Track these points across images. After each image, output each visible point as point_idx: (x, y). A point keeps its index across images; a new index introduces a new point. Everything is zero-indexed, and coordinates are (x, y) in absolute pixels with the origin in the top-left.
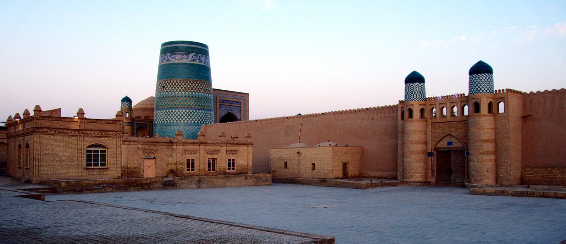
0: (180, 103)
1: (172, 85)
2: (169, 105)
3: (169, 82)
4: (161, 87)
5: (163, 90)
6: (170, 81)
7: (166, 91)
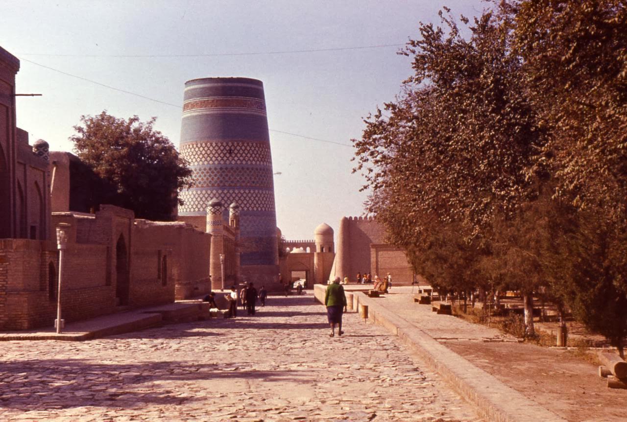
0: (259, 179)
1: (246, 149)
2: (244, 182)
3: (240, 144)
4: (225, 152)
5: (230, 156)
6: (243, 144)
7: (236, 158)
